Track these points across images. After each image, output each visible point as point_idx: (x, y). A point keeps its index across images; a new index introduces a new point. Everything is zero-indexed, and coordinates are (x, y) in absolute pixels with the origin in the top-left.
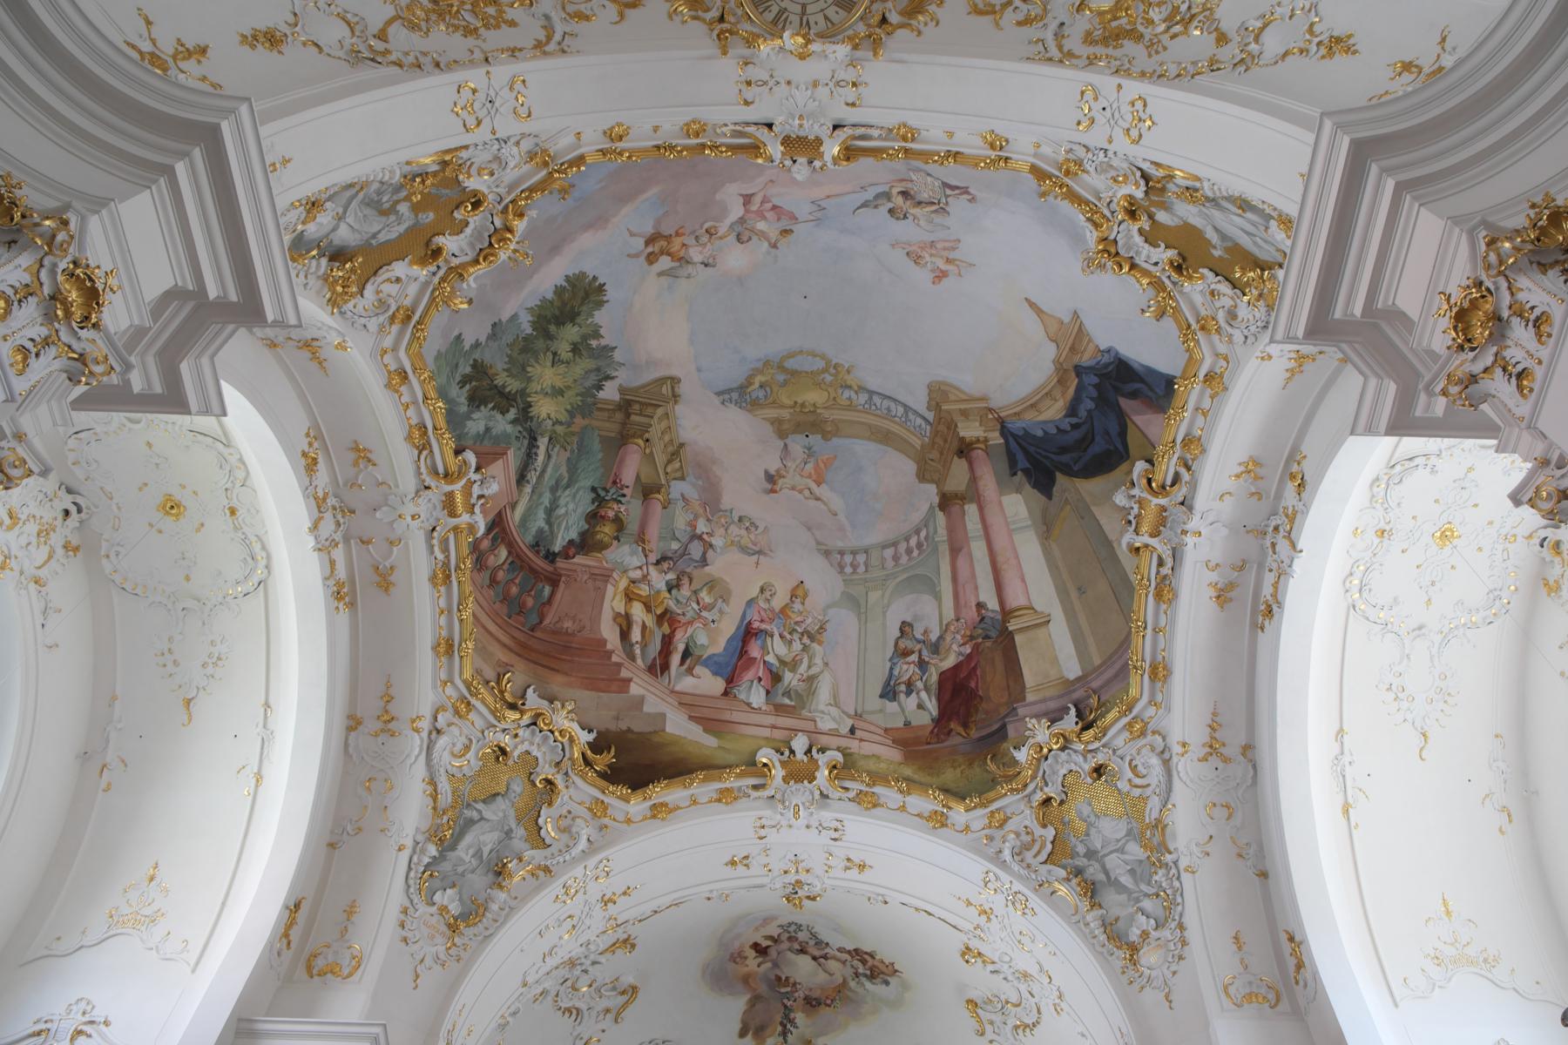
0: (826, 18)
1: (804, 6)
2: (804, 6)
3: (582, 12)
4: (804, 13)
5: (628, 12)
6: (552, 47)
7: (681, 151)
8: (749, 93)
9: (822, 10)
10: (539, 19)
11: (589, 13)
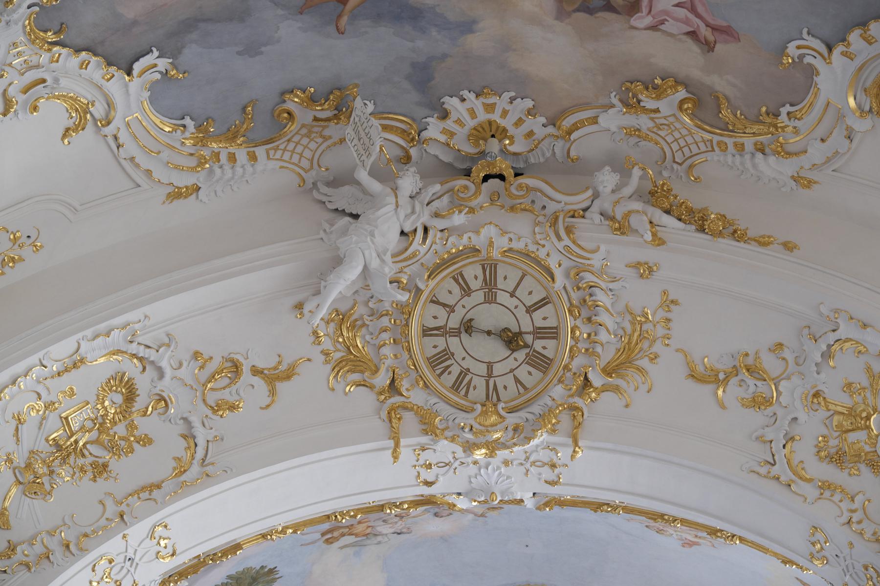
0: (517, 381)
1: (490, 366)
2: (490, 366)
3: (227, 403)
4: (490, 375)
5: (282, 387)
6: (195, 469)
7: (355, 516)
8: (429, 475)
9: (512, 371)
10: (176, 424)
11: (231, 399)
